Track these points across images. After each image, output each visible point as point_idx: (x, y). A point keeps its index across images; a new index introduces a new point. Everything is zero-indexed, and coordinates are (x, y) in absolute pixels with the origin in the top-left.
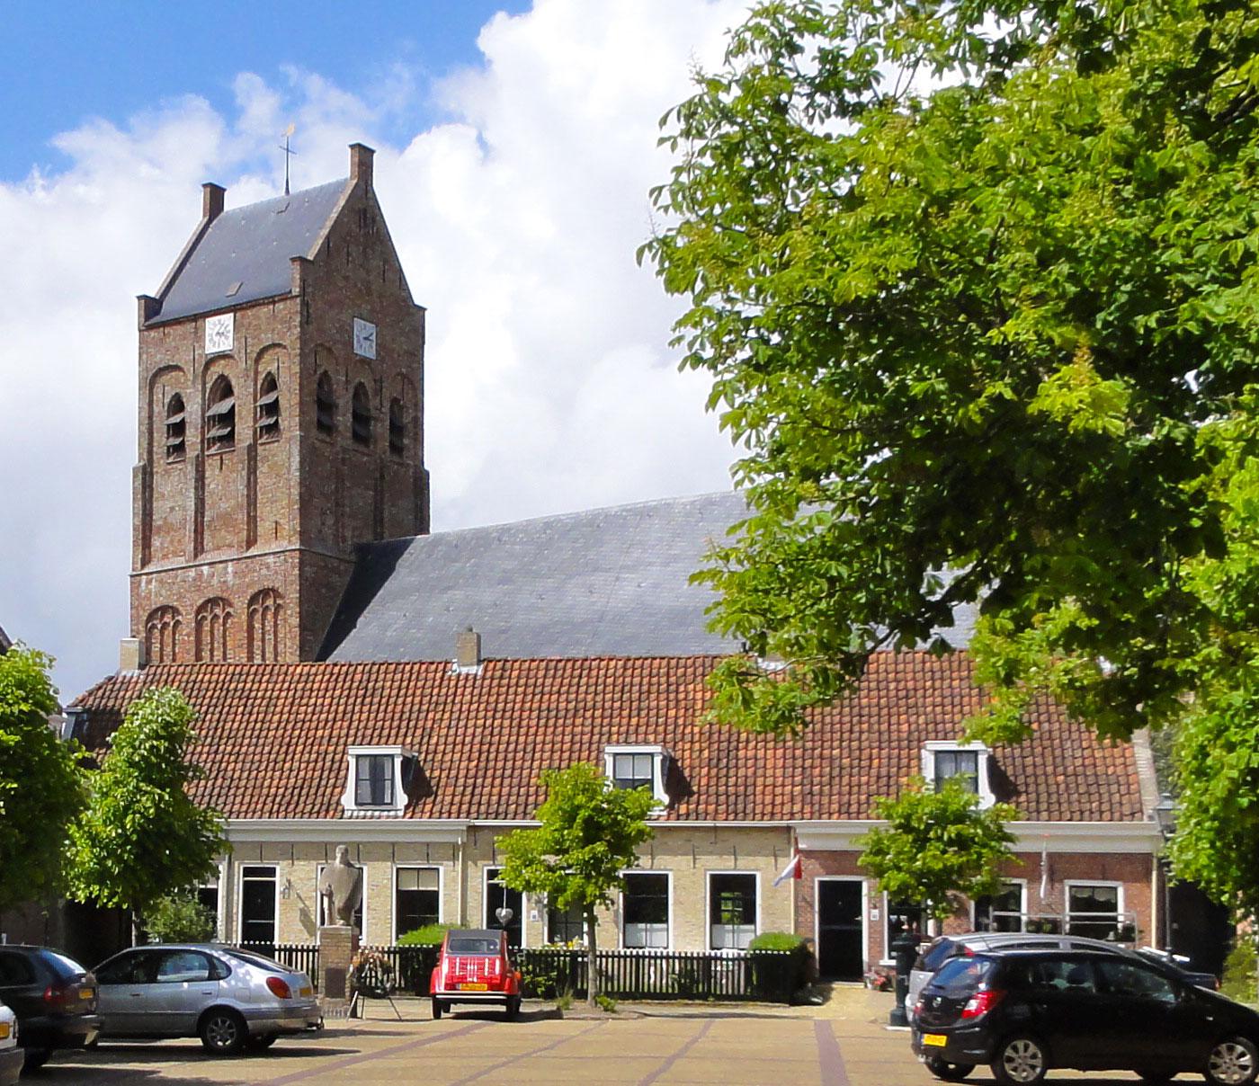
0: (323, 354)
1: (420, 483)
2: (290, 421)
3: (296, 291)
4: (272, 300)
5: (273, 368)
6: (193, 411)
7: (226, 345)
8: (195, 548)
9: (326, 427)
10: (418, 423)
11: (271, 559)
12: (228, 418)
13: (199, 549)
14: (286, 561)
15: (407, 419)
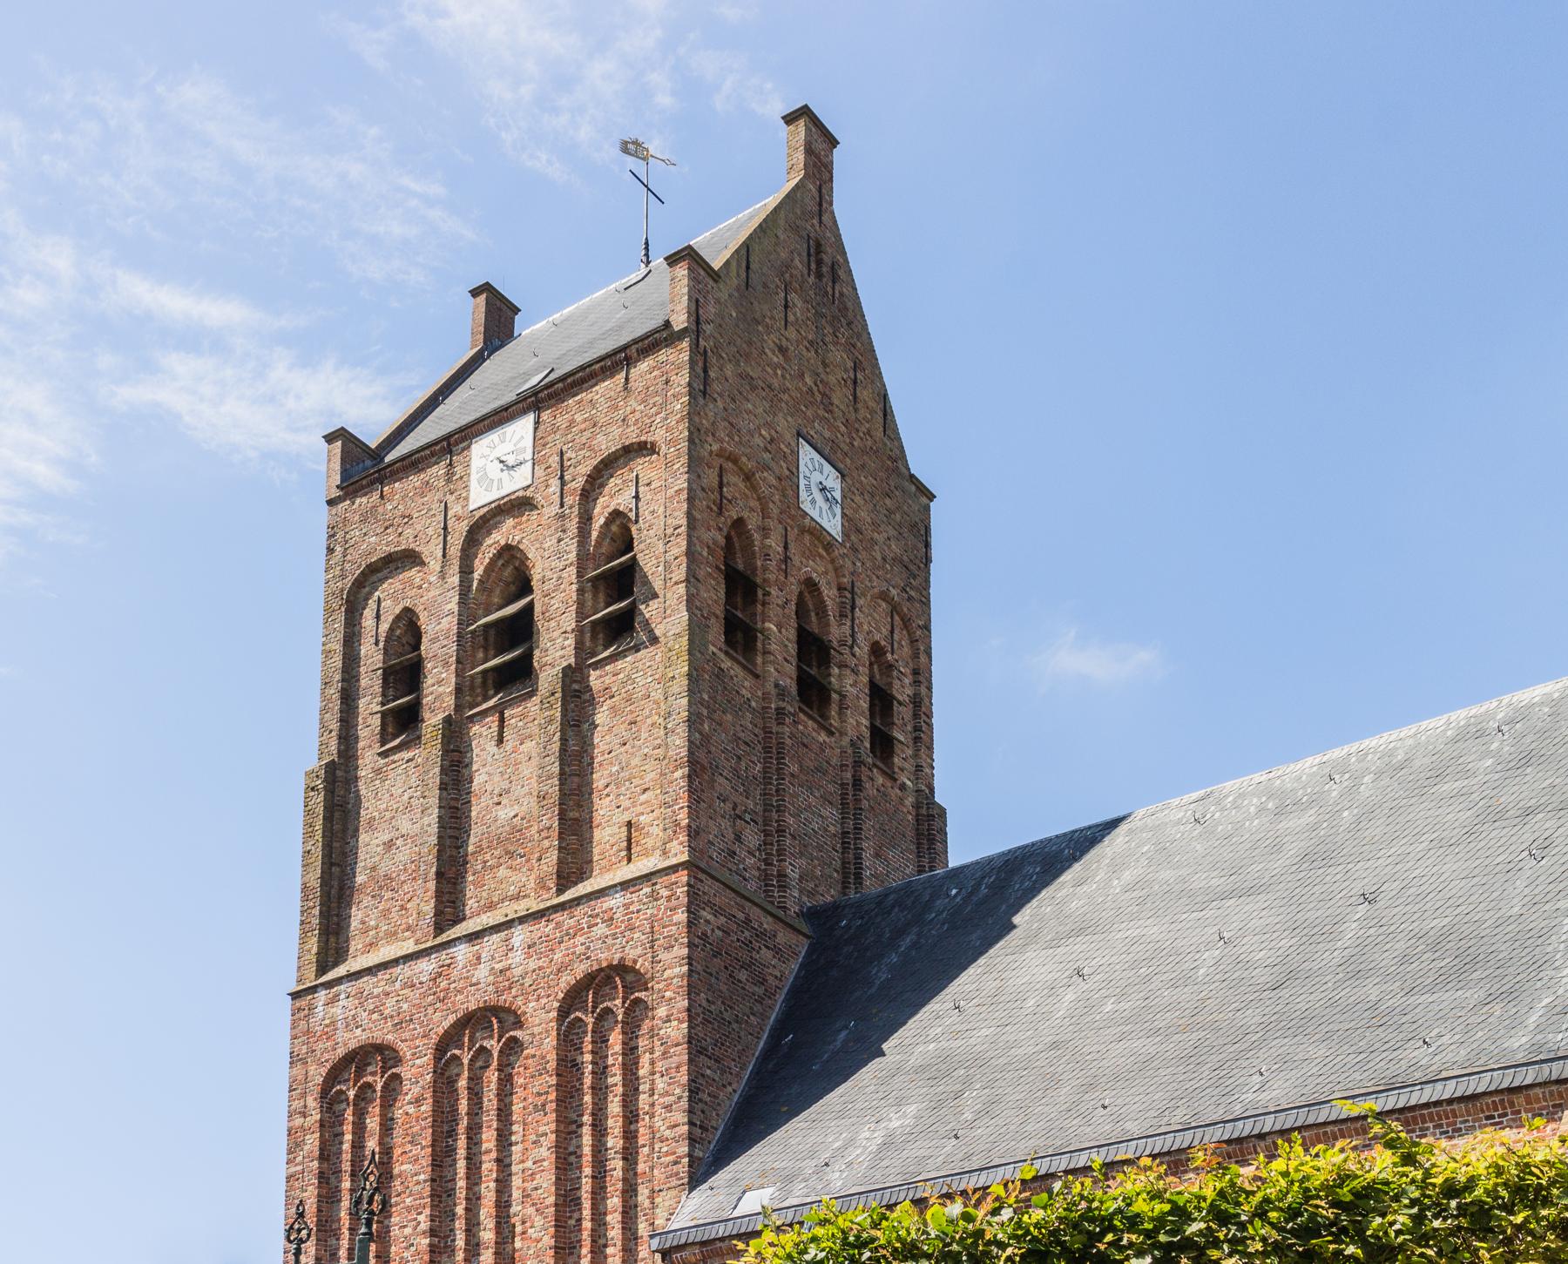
2: (668, 613)
3: (680, 321)
4: (619, 360)
5: (624, 501)
7: (515, 482)
8: (438, 913)
9: (741, 635)
10: (921, 707)
11: (615, 901)
12: (521, 630)
13: (449, 909)
14: (654, 897)
15: (902, 690)
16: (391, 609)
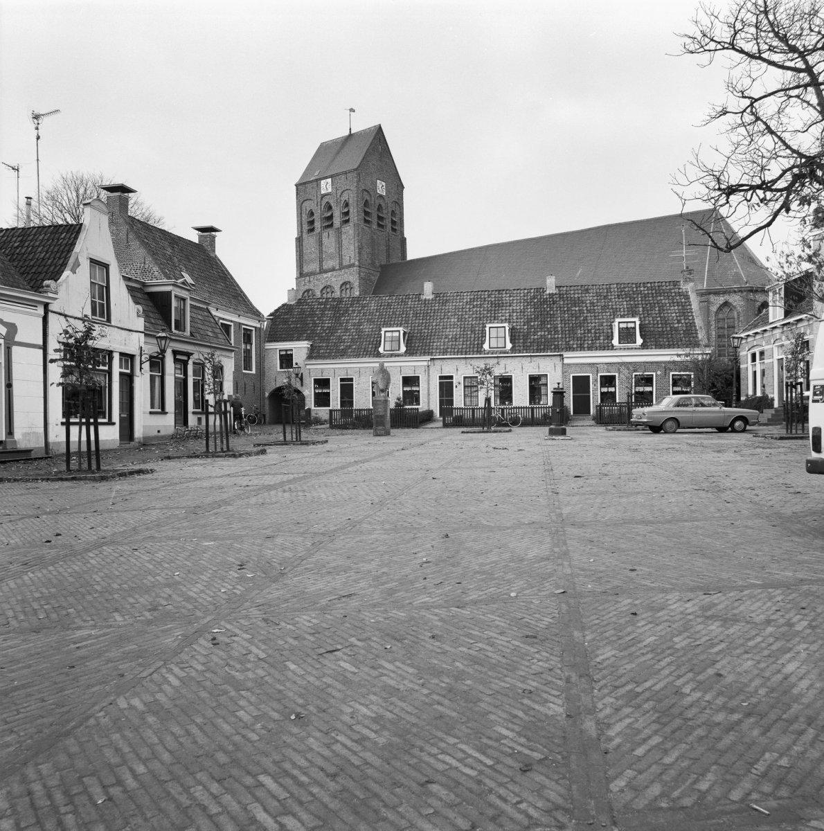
1: (403, 241)
2: (354, 215)
6: (317, 217)
12: (331, 217)
16: (308, 209)
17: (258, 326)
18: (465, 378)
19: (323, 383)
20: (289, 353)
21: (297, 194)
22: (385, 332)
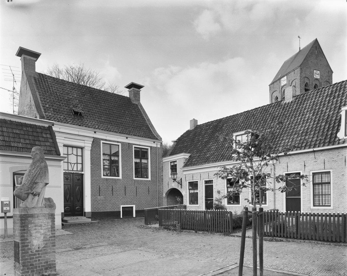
0: (306, 79)
17: (154, 145)
18: (314, 174)
19: (194, 185)
20: (175, 164)
21: (270, 90)
22: (236, 136)
